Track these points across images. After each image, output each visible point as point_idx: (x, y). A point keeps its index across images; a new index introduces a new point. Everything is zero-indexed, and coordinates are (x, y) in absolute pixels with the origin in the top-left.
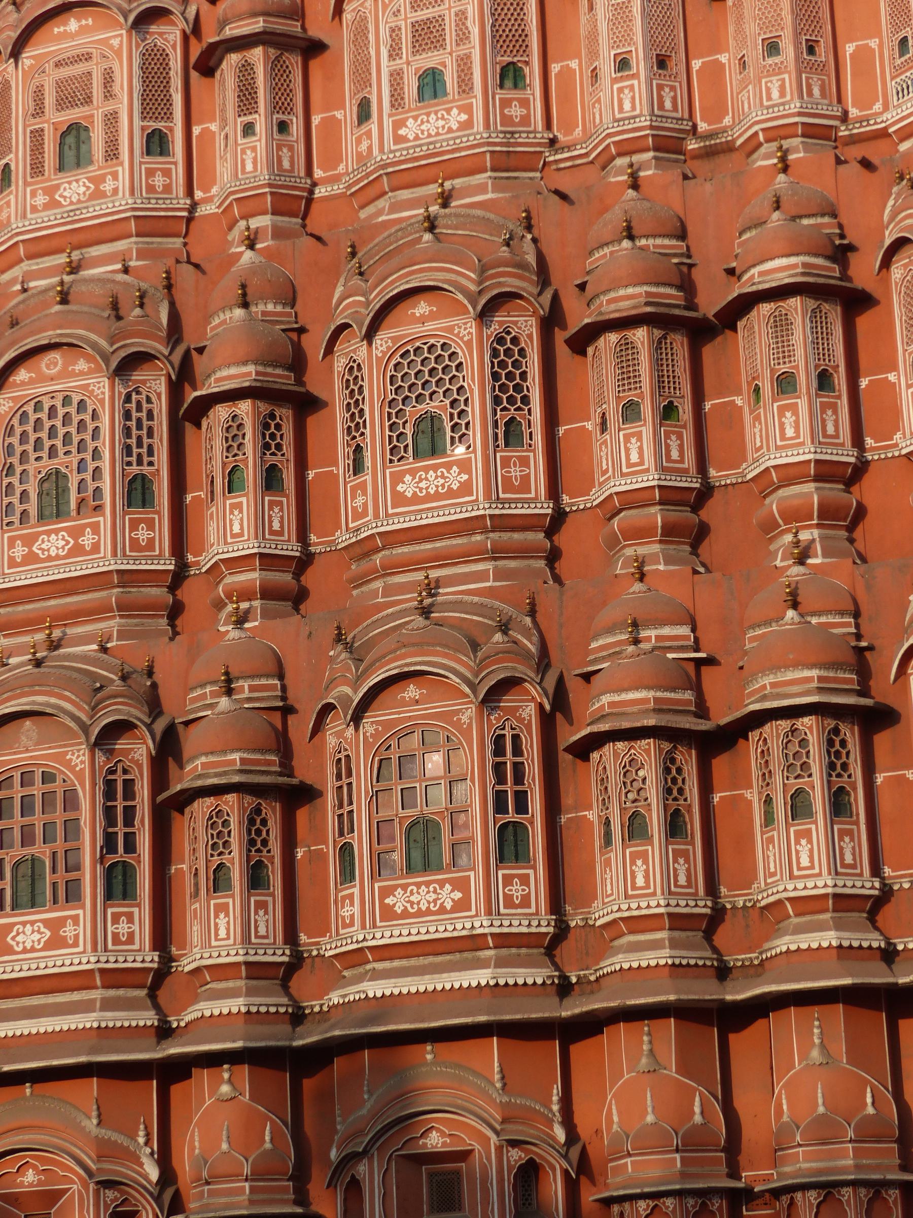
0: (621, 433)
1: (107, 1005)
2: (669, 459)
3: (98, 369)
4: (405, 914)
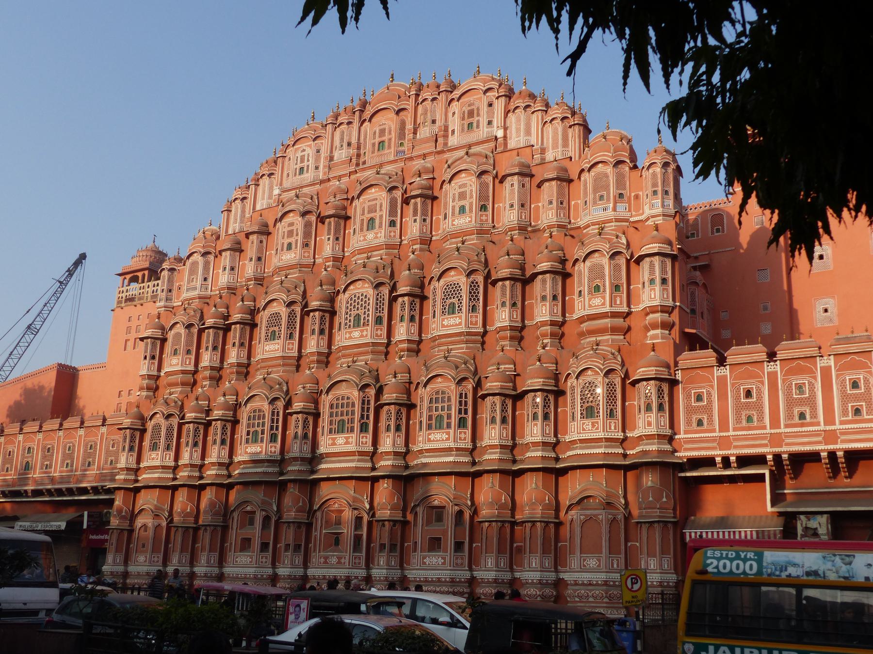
1: (359, 461)
4: (434, 441)
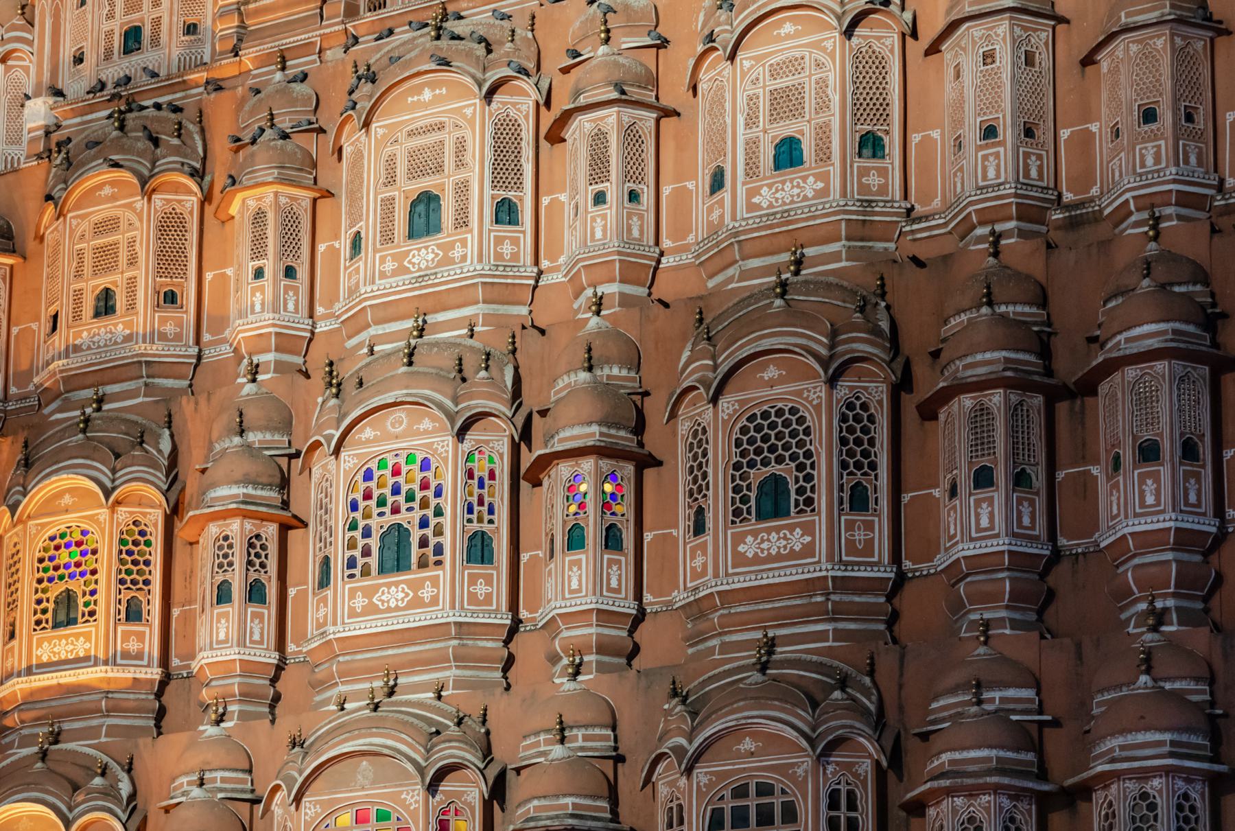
0: (972, 499)
2: (1020, 525)
3: (442, 429)
